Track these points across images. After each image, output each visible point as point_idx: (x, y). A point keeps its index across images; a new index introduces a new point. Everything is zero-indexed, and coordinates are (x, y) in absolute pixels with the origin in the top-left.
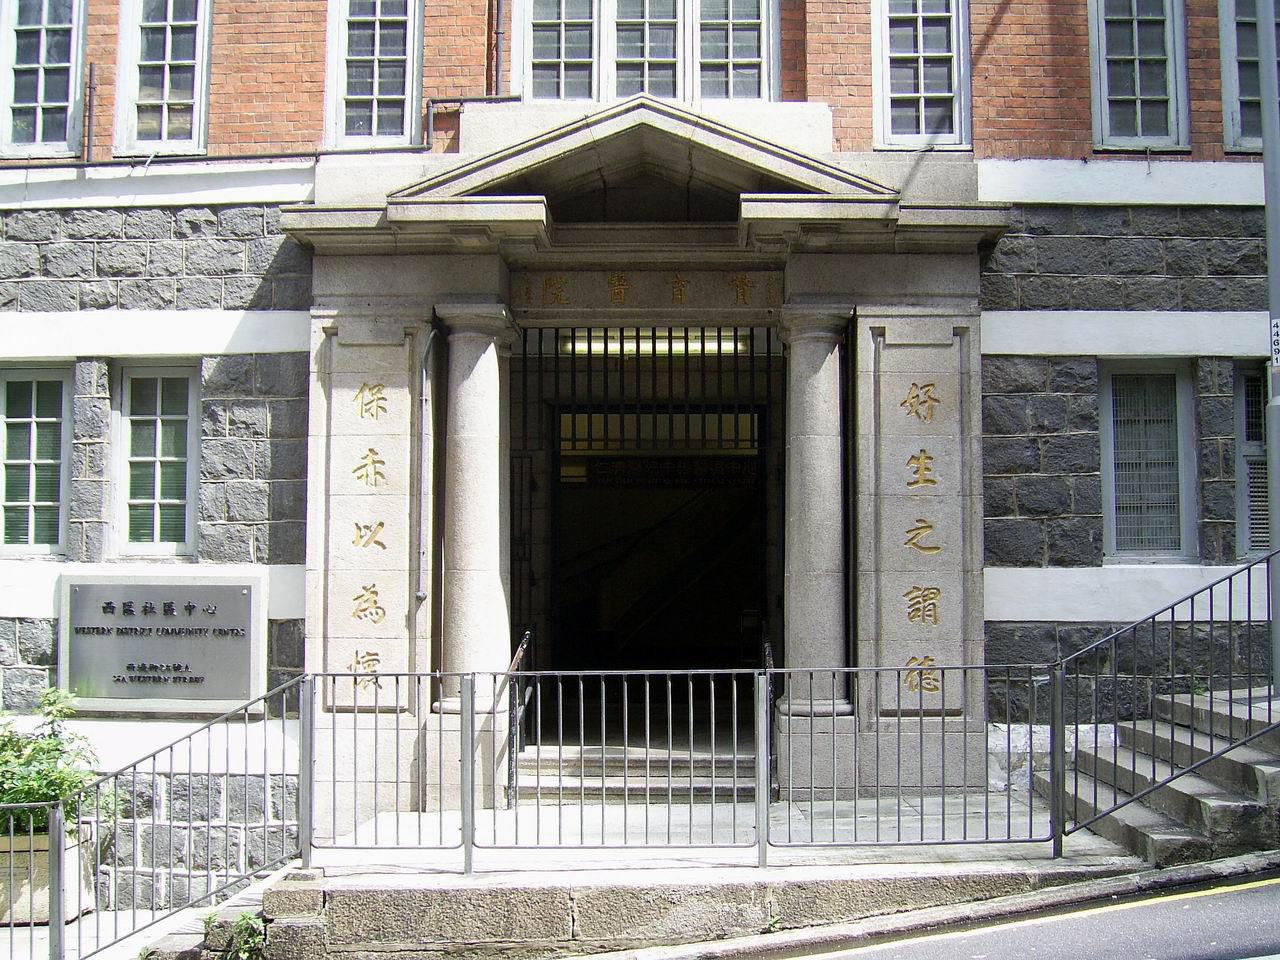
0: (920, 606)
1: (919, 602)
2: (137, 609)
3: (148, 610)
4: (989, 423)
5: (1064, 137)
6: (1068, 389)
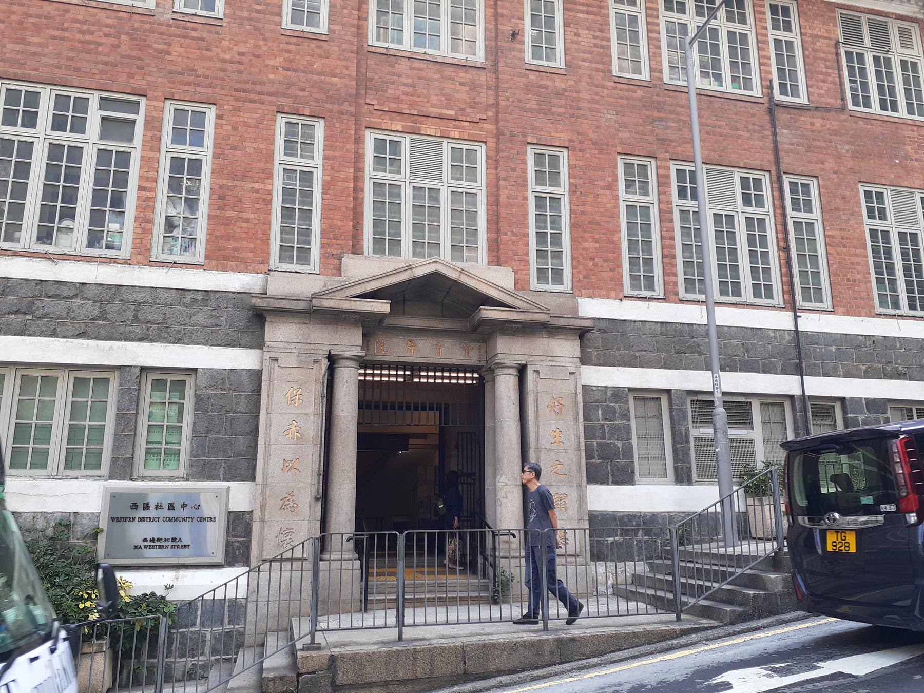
2: (152, 506)
3: (158, 507)
4: (586, 418)
5: (612, 289)
6: (616, 402)
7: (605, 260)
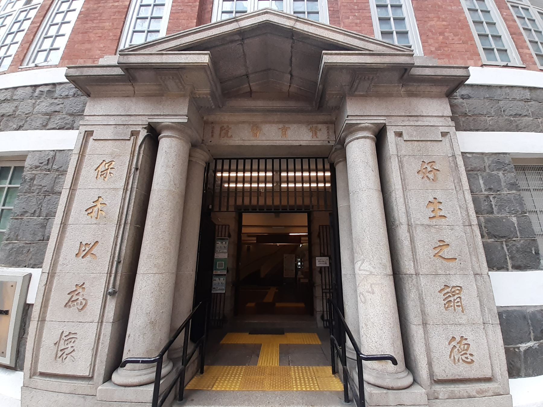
0: (452, 299)
1: (450, 296)
7: (456, 35)
